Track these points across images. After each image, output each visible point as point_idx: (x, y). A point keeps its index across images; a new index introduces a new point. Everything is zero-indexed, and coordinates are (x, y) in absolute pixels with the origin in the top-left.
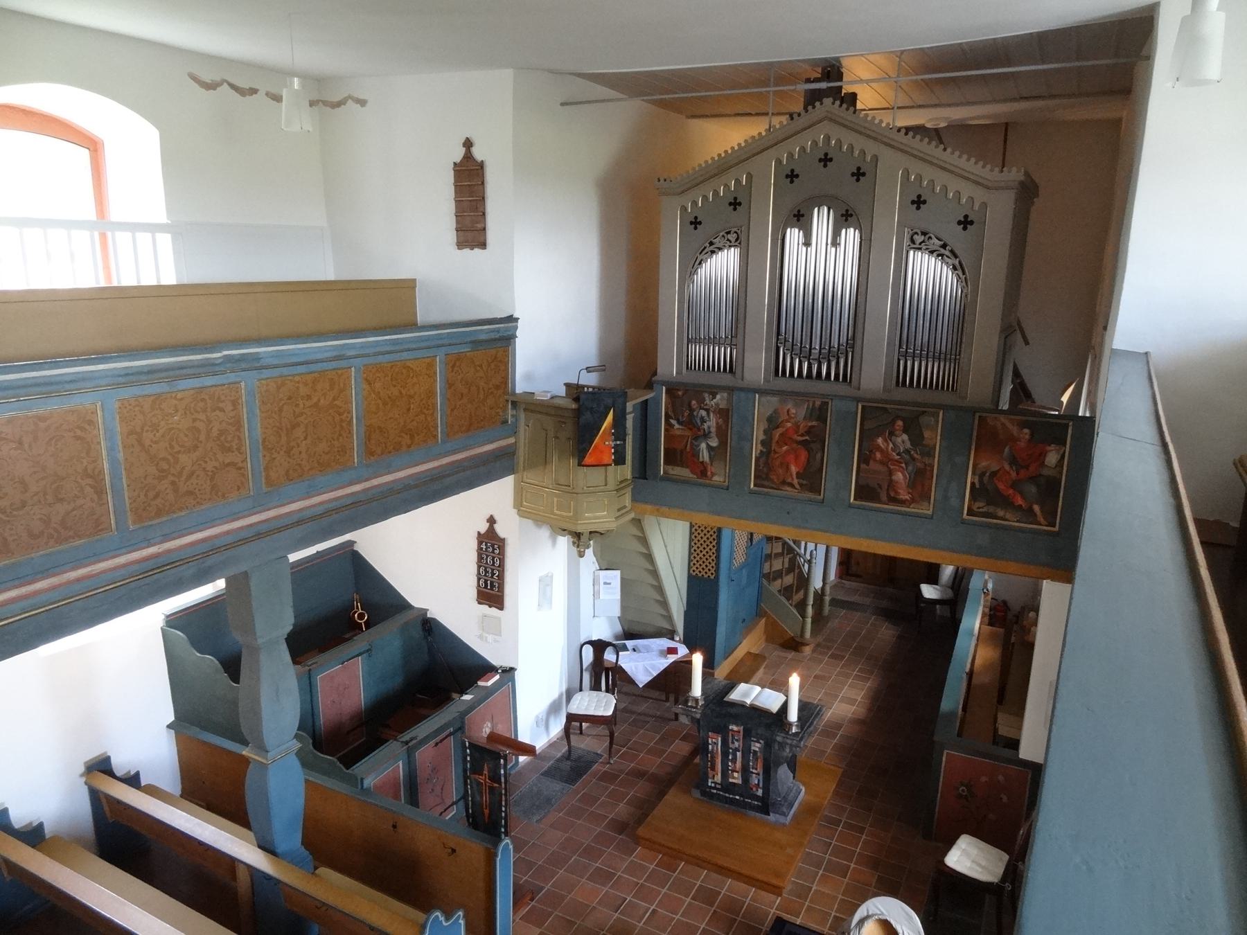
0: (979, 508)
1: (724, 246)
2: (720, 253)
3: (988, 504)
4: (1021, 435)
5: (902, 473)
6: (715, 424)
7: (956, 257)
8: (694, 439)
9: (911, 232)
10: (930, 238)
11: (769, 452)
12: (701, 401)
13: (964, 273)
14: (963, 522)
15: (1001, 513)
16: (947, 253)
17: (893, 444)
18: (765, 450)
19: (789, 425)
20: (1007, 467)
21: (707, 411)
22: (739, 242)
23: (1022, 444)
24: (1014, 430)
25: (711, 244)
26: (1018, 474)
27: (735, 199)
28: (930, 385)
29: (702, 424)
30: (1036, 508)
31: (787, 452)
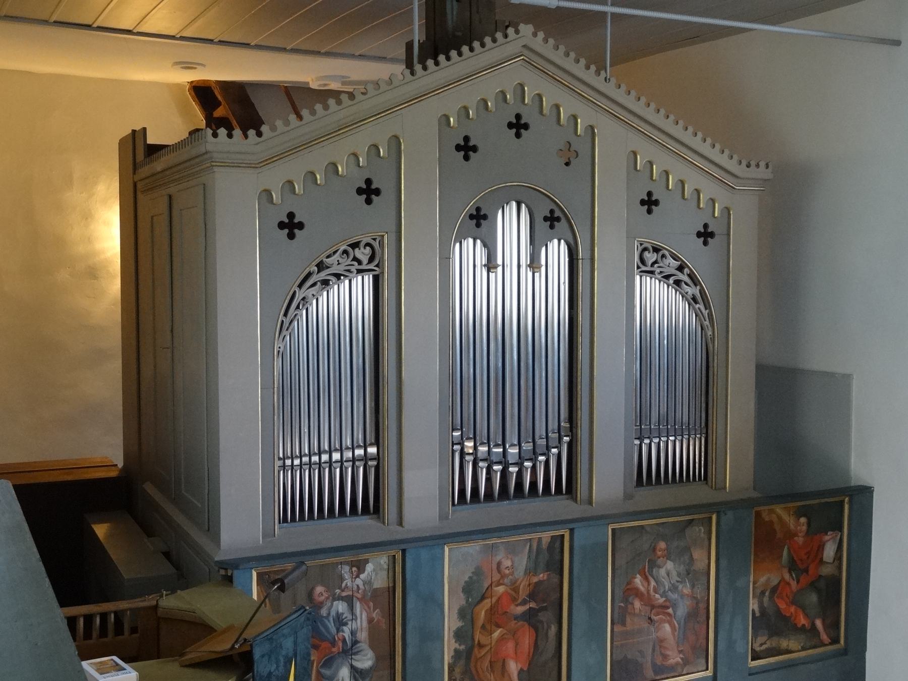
0: (761, 645)
1: (349, 271)
2: (336, 287)
3: (770, 636)
4: (799, 528)
5: (670, 625)
6: (365, 624)
7: (696, 282)
8: (322, 667)
9: (640, 248)
10: (663, 256)
11: (469, 652)
12: (332, 581)
13: (707, 306)
14: (753, 673)
15: (784, 644)
16: (686, 278)
17: (656, 582)
18: (462, 647)
19: (501, 589)
20: (787, 576)
21: (349, 600)
22: (376, 262)
23: (800, 540)
24: (790, 521)
25: (321, 266)
26: (798, 582)
27: (368, 182)
28: (679, 478)
29: (338, 630)
30: (819, 623)
31: (502, 639)
